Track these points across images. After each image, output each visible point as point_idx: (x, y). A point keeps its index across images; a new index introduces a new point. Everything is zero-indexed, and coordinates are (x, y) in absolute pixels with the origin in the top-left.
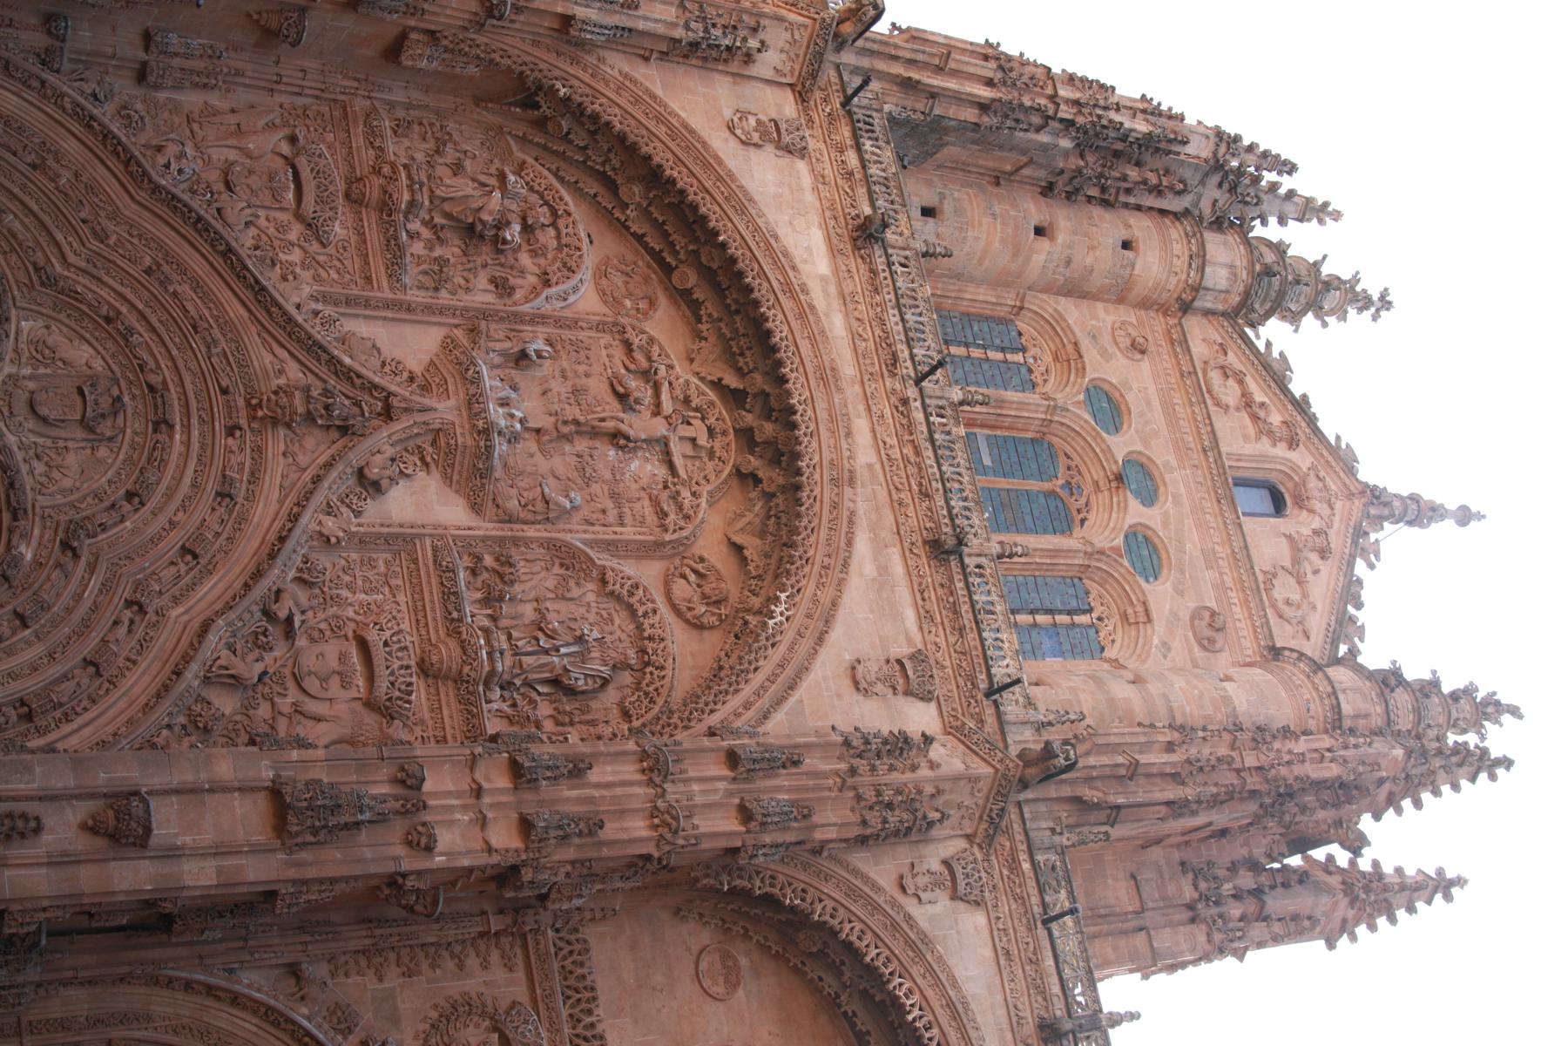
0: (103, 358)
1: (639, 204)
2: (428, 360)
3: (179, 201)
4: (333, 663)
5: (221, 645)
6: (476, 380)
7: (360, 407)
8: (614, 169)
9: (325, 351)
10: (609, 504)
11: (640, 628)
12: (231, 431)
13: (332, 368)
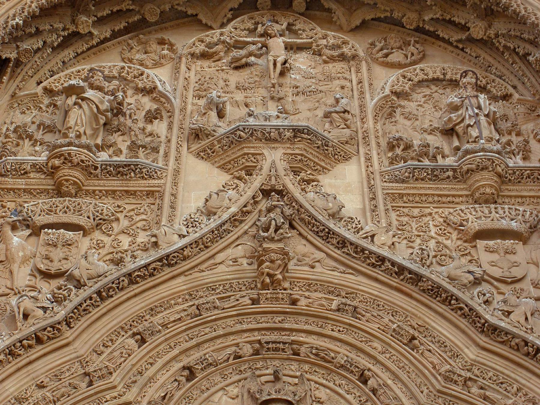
0: (227, 386)
1: (94, 22)
2: (216, 171)
3: (80, 305)
4: (495, 257)
5: (507, 320)
6: (252, 132)
7: (275, 207)
8: (64, 29)
9: (224, 224)
10: (337, 82)
11: (435, 81)
12: (294, 302)
13: (237, 223)
